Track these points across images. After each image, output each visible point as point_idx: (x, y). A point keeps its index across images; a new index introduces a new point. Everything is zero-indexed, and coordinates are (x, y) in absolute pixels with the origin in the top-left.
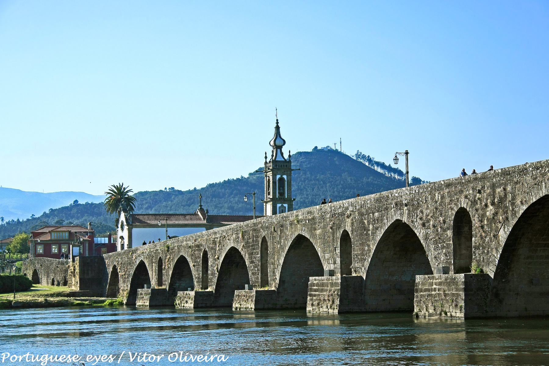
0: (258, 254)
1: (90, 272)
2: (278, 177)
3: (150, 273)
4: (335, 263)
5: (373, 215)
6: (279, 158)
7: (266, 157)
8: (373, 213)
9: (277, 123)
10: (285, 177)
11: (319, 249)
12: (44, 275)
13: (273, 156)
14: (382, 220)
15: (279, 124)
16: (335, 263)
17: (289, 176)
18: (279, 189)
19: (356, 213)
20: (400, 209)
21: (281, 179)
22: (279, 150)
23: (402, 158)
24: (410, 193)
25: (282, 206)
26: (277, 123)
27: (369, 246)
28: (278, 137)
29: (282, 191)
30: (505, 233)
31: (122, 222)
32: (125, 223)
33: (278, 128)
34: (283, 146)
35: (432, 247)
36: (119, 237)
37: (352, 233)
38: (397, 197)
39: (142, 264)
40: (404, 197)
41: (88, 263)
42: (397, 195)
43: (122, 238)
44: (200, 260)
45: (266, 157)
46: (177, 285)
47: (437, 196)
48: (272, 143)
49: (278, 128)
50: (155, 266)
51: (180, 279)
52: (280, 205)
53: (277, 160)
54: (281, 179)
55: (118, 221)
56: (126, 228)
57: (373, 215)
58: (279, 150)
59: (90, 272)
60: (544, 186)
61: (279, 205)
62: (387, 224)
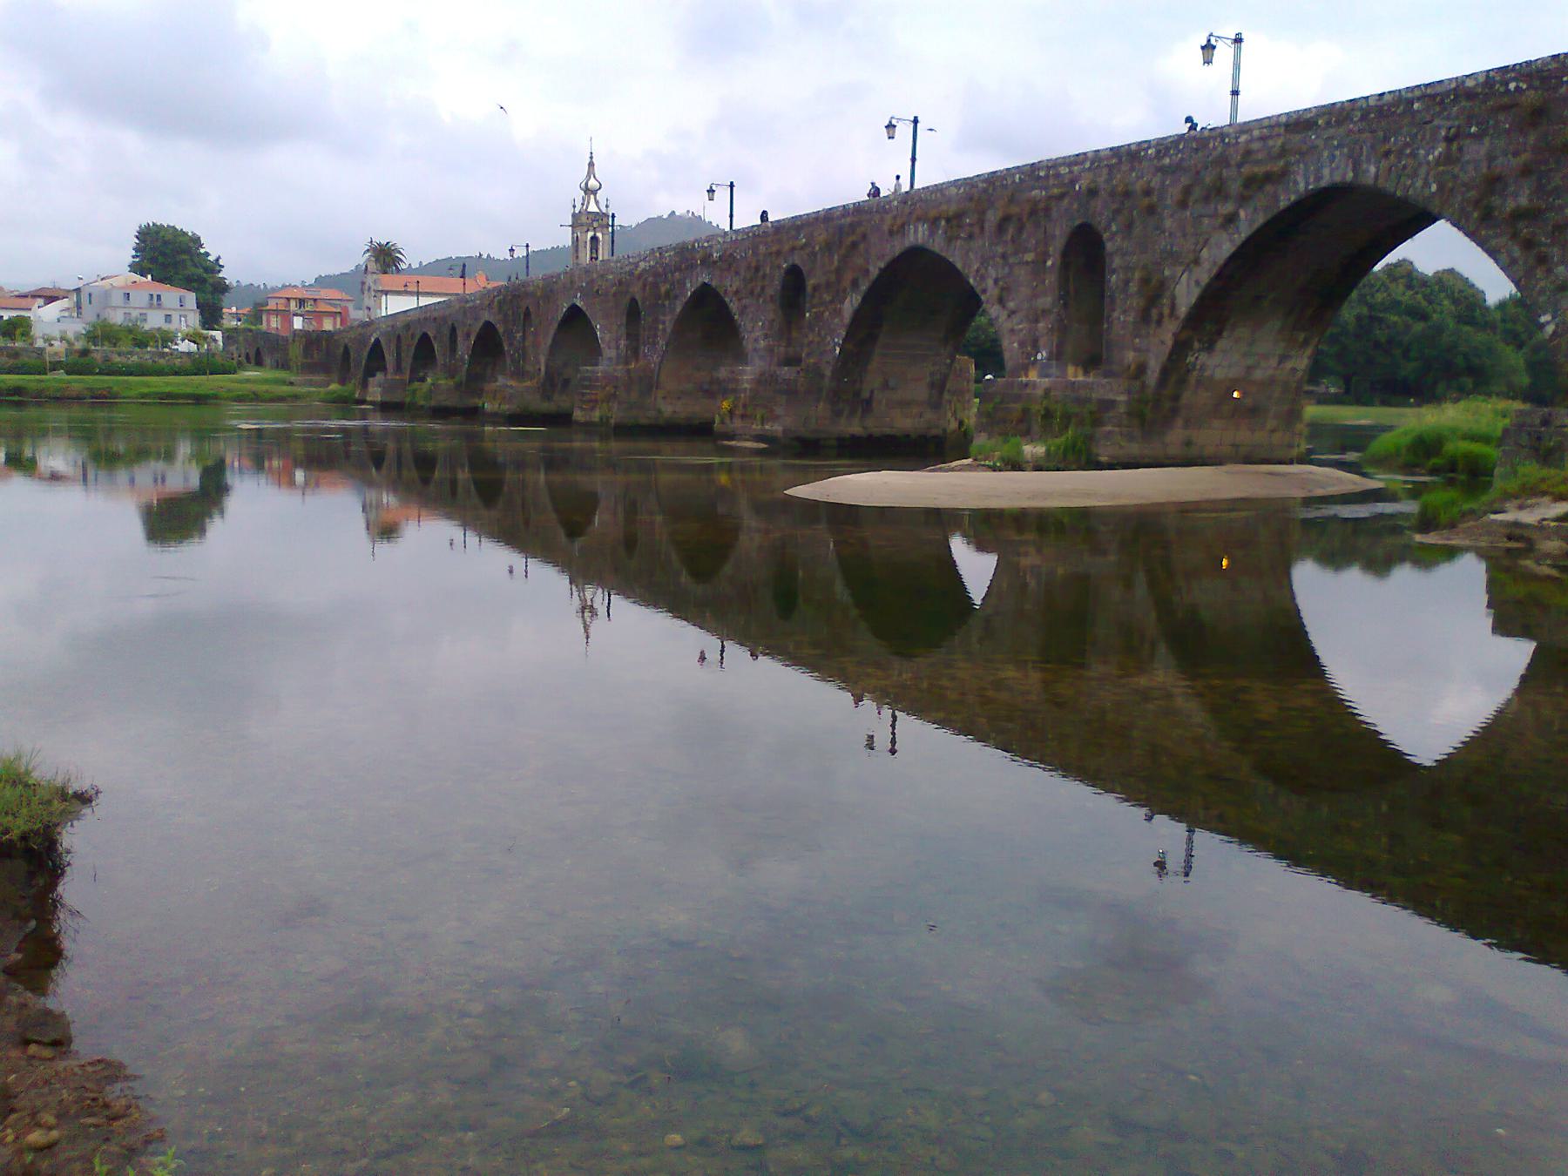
0: (519, 332)
2: (590, 234)
3: (387, 356)
4: (618, 348)
5: (672, 276)
6: (593, 208)
7: (574, 206)
9: (591, 158)
10: (599, 235)
11: (598, 327)
13: (583, 204)
14: (685, 284)
15: (594, 160)
16: (618, 348)
18: (591, 253)
21: (594, 238)
22: (592, 196)
23: (722, 195)
26: (591, 158)
28: (592, 176)
29: (594, 255)
30: (852, 305)
33: (591, 164)
34: (599, 192)
37: (643, 303)
38: (706, 248)
39: (377, 341)
42: (706, 244)
44: (446, 339)
45: (574, 206)
48: (583, 185)
49: (591, 164)
50: (393, 347)
53: (589, 210)
57: (672, 276)
58: (592, 196)
60: (912, 231)
62: (690, 290)
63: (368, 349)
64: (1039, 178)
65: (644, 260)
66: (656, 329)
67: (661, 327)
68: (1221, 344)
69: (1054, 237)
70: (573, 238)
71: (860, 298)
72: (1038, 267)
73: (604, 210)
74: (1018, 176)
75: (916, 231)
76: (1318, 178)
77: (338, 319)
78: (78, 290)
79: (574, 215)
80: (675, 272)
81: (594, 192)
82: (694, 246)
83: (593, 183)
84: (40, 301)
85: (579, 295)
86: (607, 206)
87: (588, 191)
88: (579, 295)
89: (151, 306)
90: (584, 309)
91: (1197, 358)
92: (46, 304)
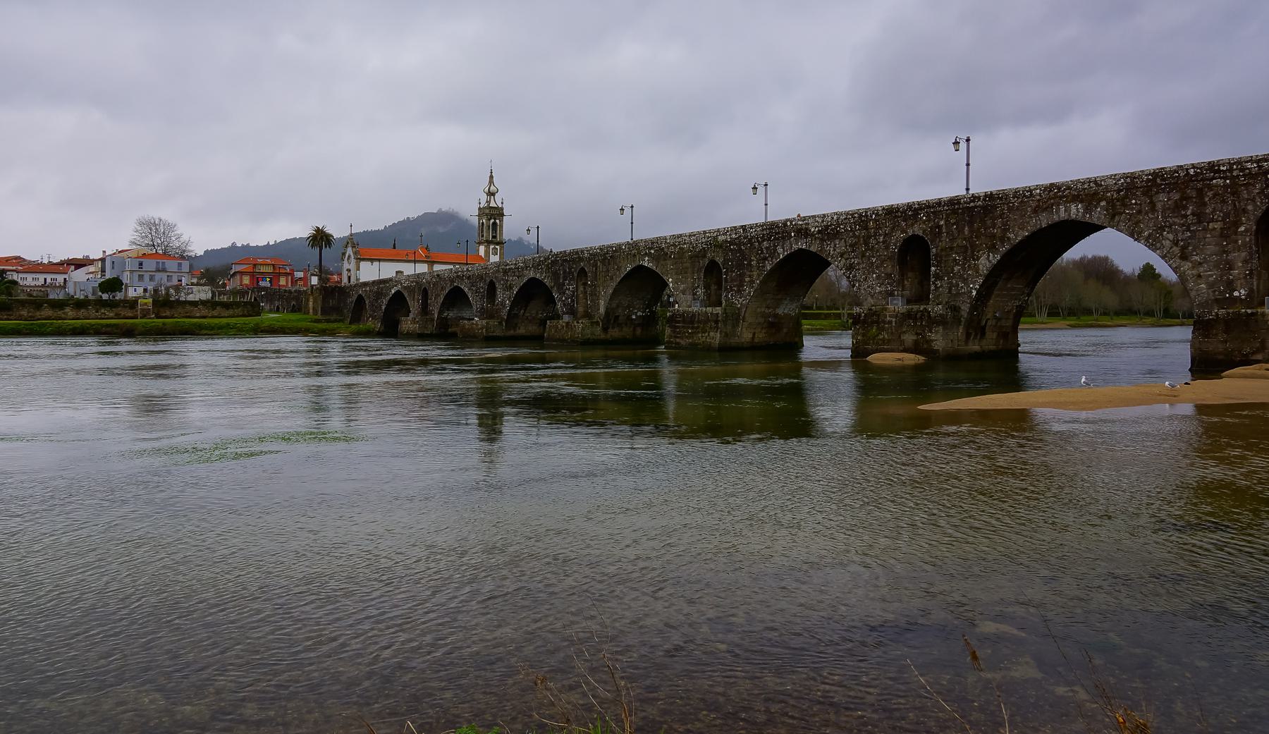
2: (492, 221)
6: (493, 205)
7: (480, 203)
10: (498, 221)
11: (670, 280)
17: (501, 221)
21: (495, 224)
24: (823, 221)
29: (494, 235)
31: (349, 256)
32: (353, 257)
33: (491, 177)
36: (345, 270)
39: (398, 293)
43: (349, 270)
45: (480, 203)
46: (445, 314)
49: (491, 177)
54: (495, 224)
55: (344, 254)
56: (353, 260)
61: (492, 247)
62: (782, 253)
63: (388, 298)
64: (1219, 171)
65: (725, 234)
69: (1245, 211)
70: (479, 223)
71: (999, 258)
72: (1228, 233)
73: (500, 206)
74: (1192, 170)
77: (290, 278)
78: (103, 260)
79: (480, 209)
80: (763, 241)
81: (493, 194)
83: (492, 188)
84: (73, 267)
85: (646, 258)
86: (502, 203)
87: (491, 194)
89: (158, 270)
92: (75, 269)
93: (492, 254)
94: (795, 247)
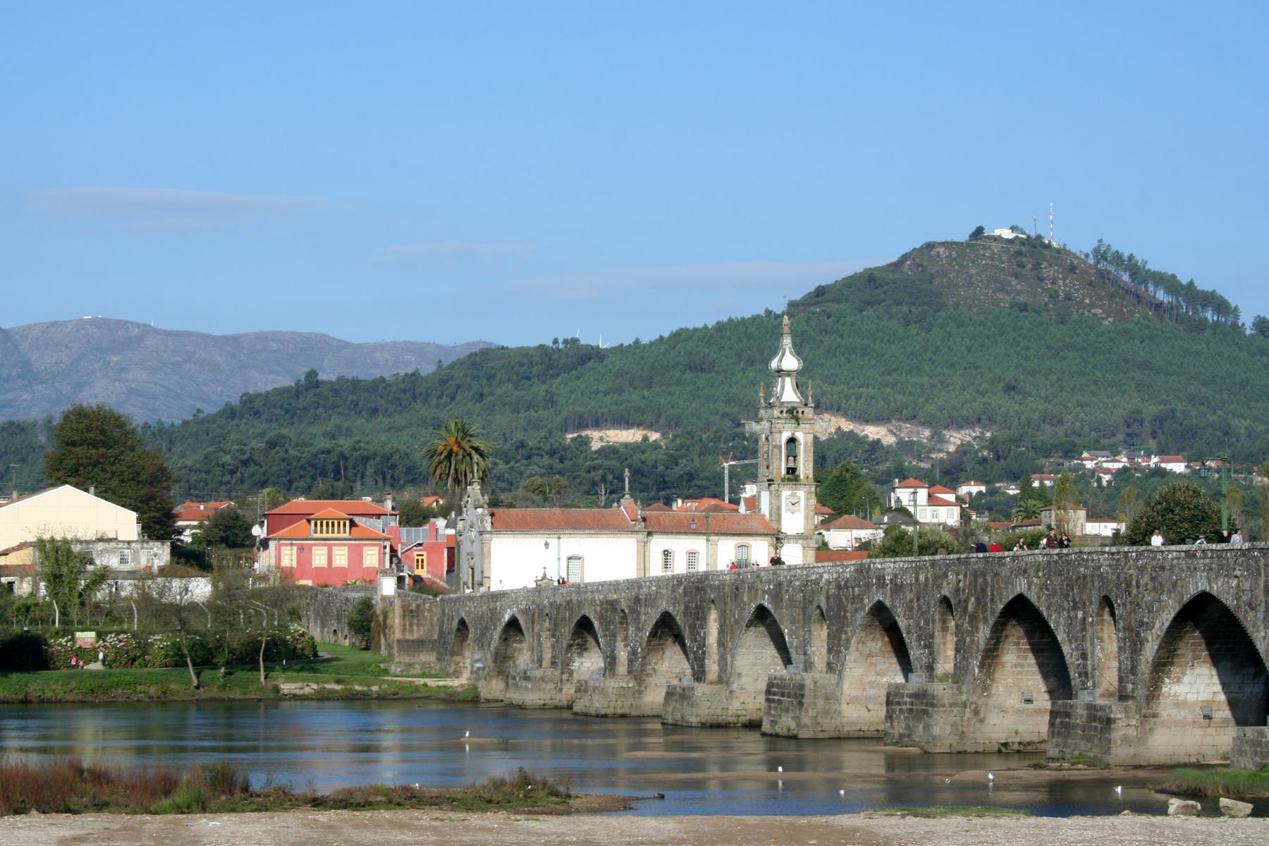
1: (415, 628)
5: (853, 590)
8: (853, 588)
11: (786, 631)
12: (316, 622)
14: (862, 600)
19: (834, 584)
20: (883, 587)
21: (792, 441)
25: (793, 495)
27: (846, 633)
29: (791, 465)
35: (914, 644)
40: (887, 570)
41: (412, 611)
42: (879, 566)
46: (576, 664)
47: (922, 578)
51: (580, 655)
52: (790, 492)
57: (853, 590)
59: (415, 628)
66: (840, 638)
67: (844, 636)
68: (1186, 679)
75: (1020, 584)
76: (1197, 587)
82: (869, 567)
88: (767, 596)
90: (772, 611)
91: (1170, 689)
93: (788, 510)
94: (876, 599)
